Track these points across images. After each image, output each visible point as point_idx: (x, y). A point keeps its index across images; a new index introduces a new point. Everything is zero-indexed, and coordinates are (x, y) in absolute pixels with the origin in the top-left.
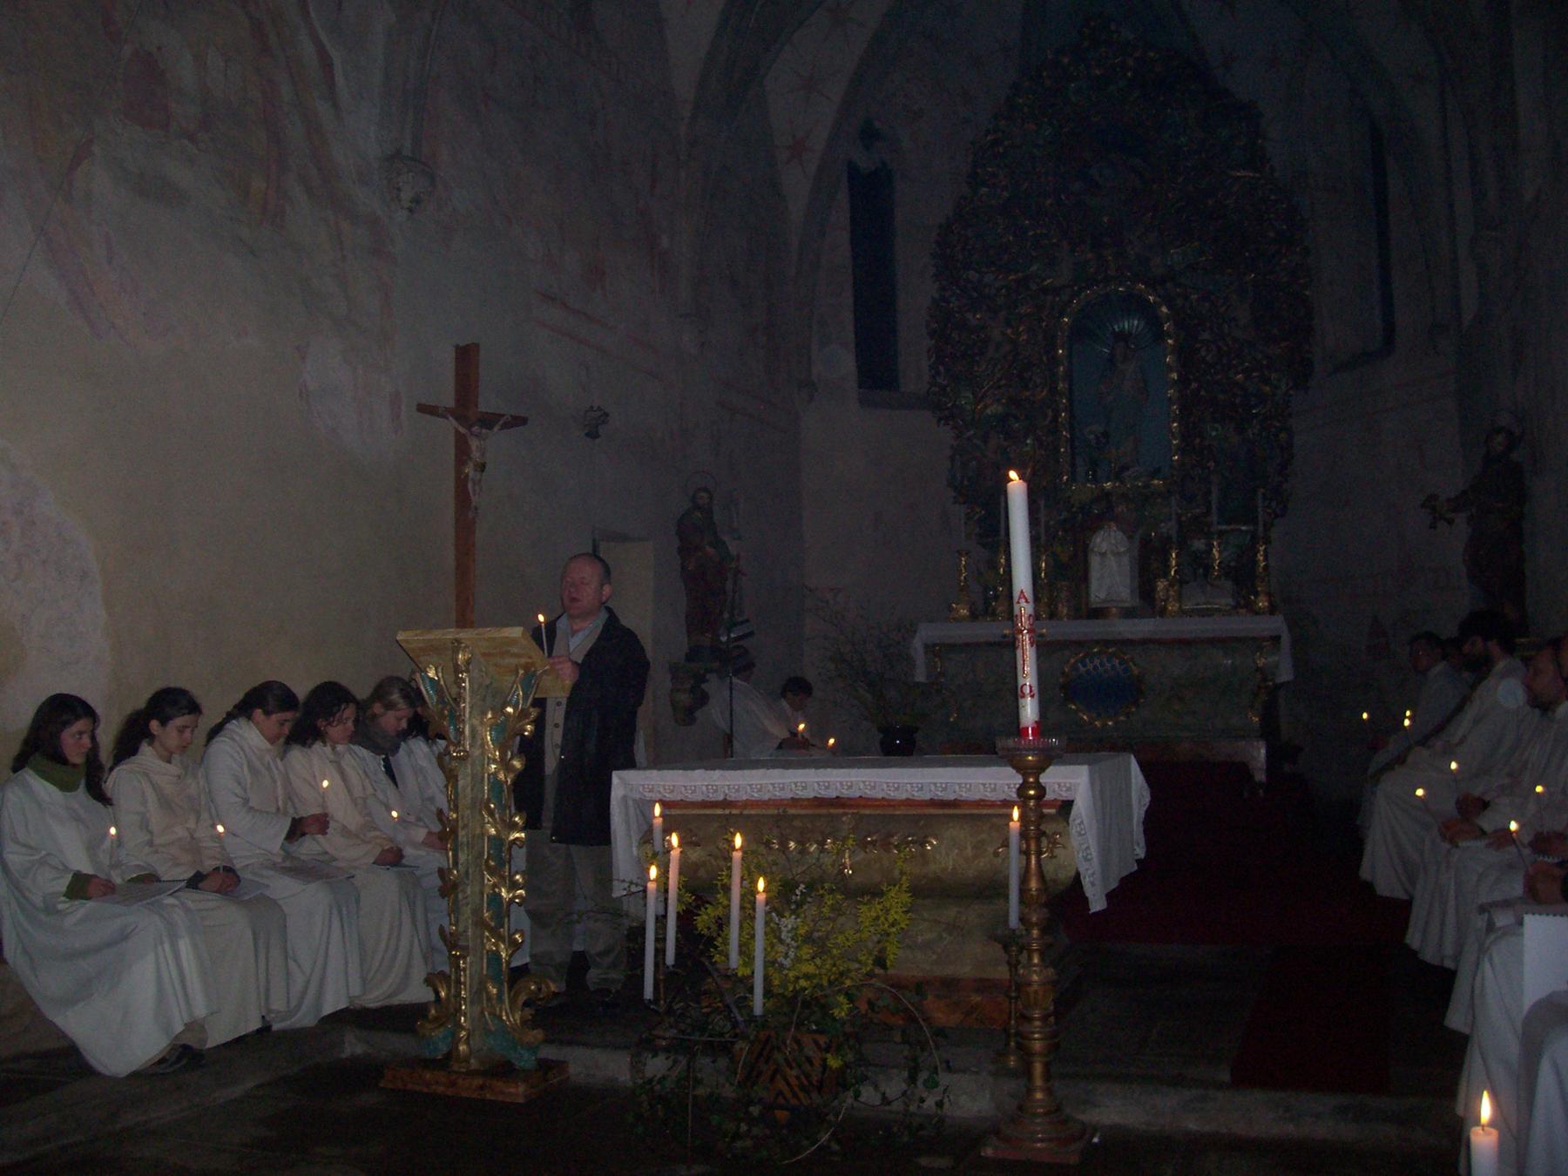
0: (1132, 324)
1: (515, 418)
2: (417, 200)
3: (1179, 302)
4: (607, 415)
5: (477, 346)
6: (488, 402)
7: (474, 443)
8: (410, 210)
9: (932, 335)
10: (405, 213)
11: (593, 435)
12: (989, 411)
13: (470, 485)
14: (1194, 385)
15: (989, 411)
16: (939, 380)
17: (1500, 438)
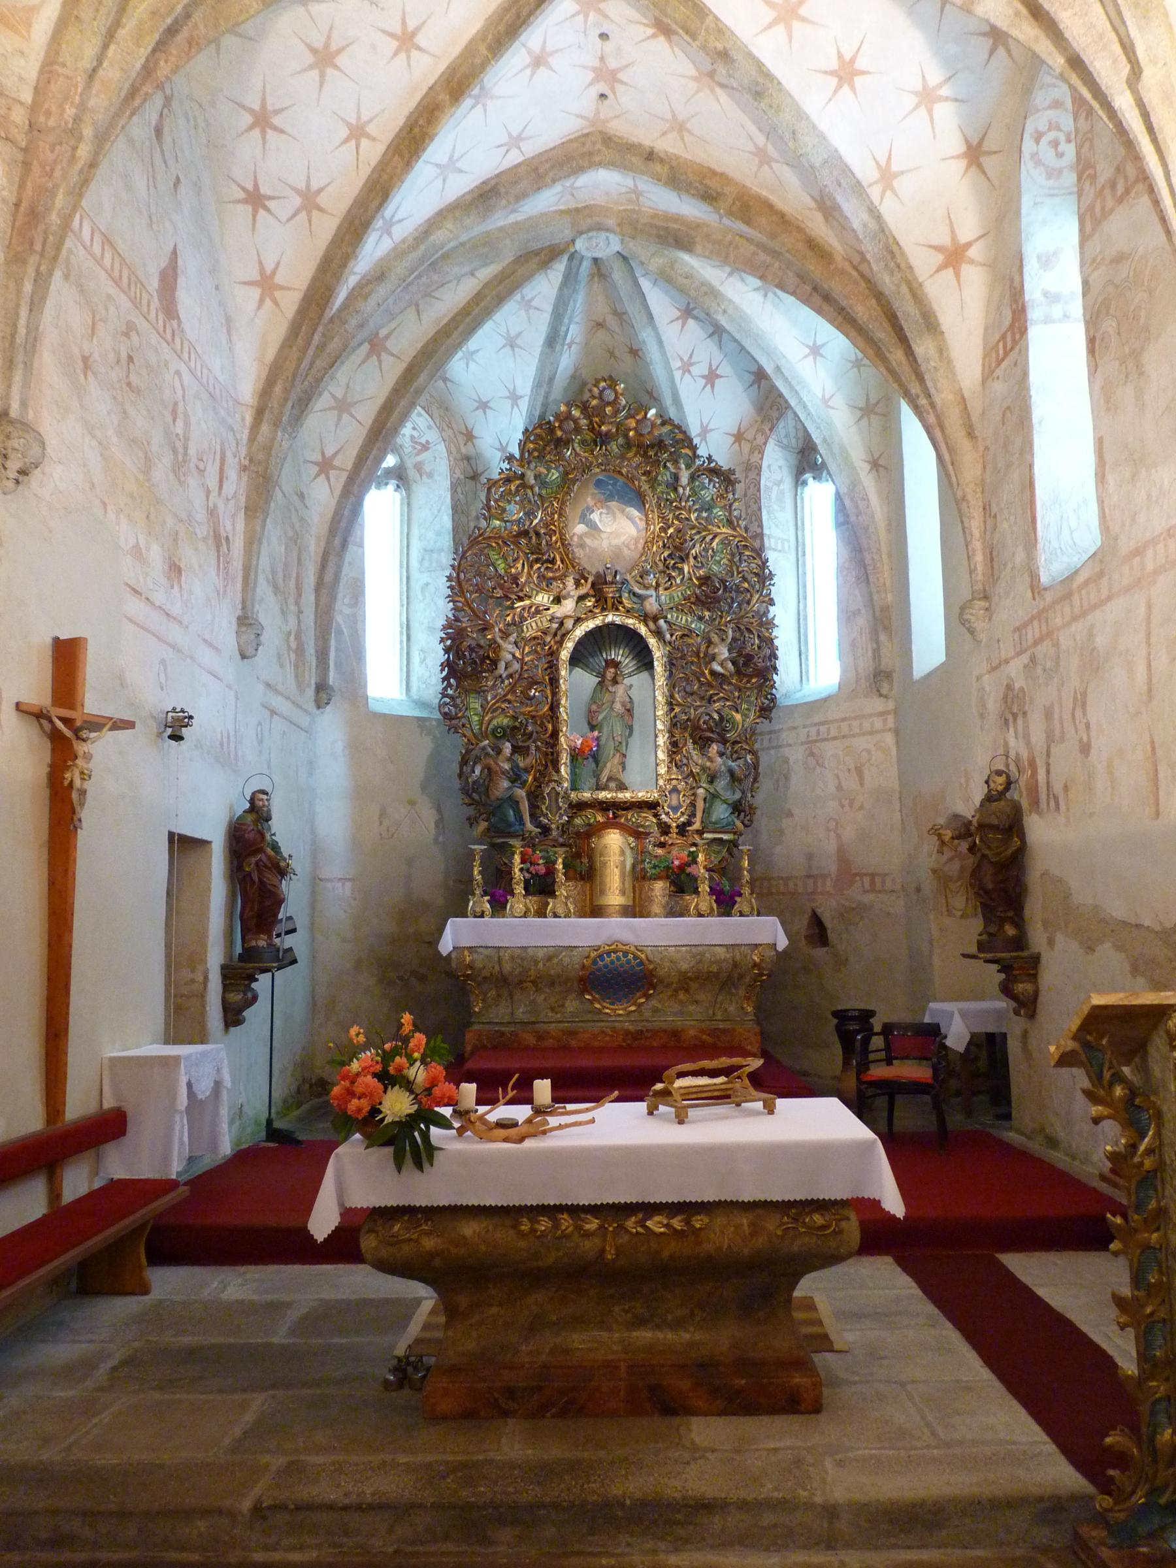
0: (619, 654)
1: (122, 721)
2: (23, 472)
3: (668, 636)
4: (191, 717)
5: (86, 639)
6: (93, 703)
7: (81, 748)
8: (17, 482)
9: (447, 650)
10: (10, 484)
11: (177, 737)
12: (495, 722)
13: (75, 796)
14: (677, 709)
15: (495, 722)
16: (450, 692)
17: (1001, 780)
